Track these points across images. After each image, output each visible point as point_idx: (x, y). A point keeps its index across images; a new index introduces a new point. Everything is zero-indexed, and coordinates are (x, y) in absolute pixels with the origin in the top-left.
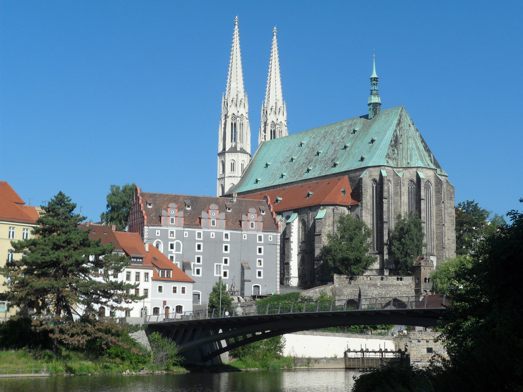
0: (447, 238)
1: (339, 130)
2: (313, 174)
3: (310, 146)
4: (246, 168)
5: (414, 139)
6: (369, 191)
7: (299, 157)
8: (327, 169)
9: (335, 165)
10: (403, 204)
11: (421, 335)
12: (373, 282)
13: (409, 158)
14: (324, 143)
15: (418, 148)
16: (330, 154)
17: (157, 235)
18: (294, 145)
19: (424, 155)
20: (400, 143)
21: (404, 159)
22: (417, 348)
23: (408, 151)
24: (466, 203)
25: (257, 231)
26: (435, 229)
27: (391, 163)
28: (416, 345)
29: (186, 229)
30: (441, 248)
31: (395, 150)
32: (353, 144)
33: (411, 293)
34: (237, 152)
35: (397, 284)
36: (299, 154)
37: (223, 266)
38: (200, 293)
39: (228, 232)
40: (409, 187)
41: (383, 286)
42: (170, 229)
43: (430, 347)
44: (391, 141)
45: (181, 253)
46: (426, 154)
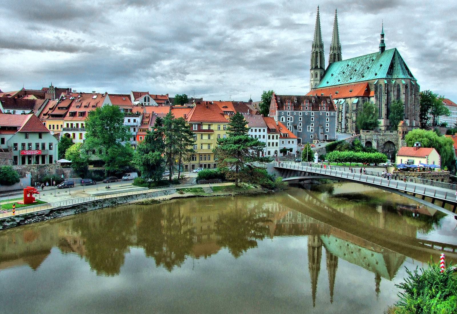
6: (378, 90)
8: (359, 78)
9: (363, 77)
12: (379, 133)
13: (398, 74)
24: (425, 91)
27: (389, 77)
34: (318, 69)
36: (346, 70)
39: (313, 112)
41: (383, 135)
42: (288, 112)
45: (292, 122)
46: (407, 71)
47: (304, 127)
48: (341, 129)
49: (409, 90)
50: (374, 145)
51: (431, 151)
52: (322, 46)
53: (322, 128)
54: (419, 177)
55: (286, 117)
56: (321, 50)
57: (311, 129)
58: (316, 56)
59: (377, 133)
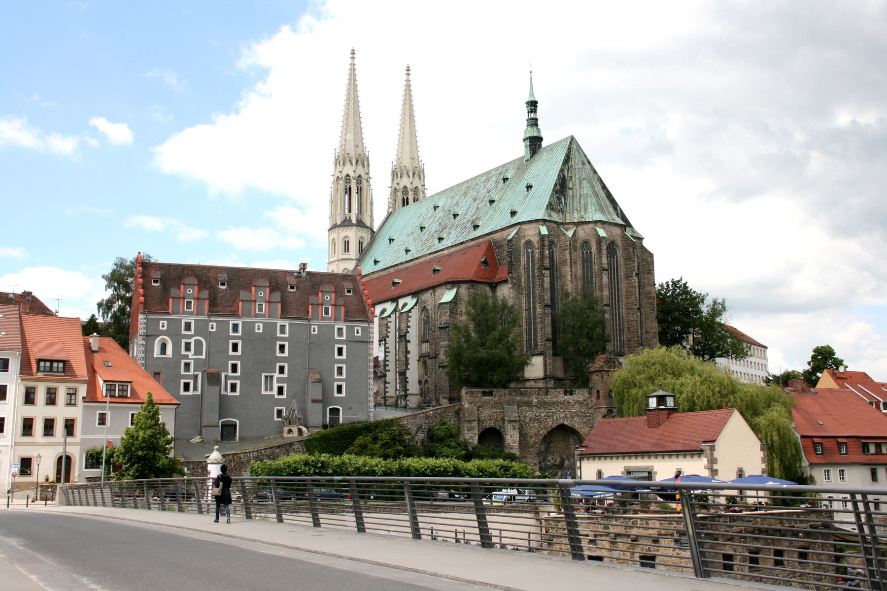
0: (644, 330)
1: (485, 182)
2: (445, 244)
3: (446, 209)
4: (365, 247)
5: (590, 182)
6: (522, 259)
7: (431, 224)
8: (464, 235)
9: (476, 227)
10: (575, 277)
12: (526, 399)
13: (583, 209)
14: (465, 201)
15: (596, 195)
16: (470, 214)
17: (161, 328)
18: (426, 211)
19: (606, 205)
20: (570, 189)
21: (576, 211)
23: (582, 198)
24: (670, 283)
25: (335, 320)
26: (625, 316)
29: (213, 319)
30: (636, 344)
31: (561, 198)
32: (502, 196)
33: (588, 415)
34: (353, 225)
35: (564, 401)
36: (431, 221)
37: (277, 378)
38: (236, 422)
39: (286, 323)
40: (583, 253)
41: (542, 405)
42: (185, 320)
44: (556, 185)
45: (203, 357)
47: (250, 379)
48: (406, 396)
49: (621, 261)
50: (512, 438)
51: (724, 422)
52: (362, 161)
53: (320, 381)
55: (176, 338)
56: (360, 171)
57: (276, 386)
58: (349, 191)
59: (518, 398)
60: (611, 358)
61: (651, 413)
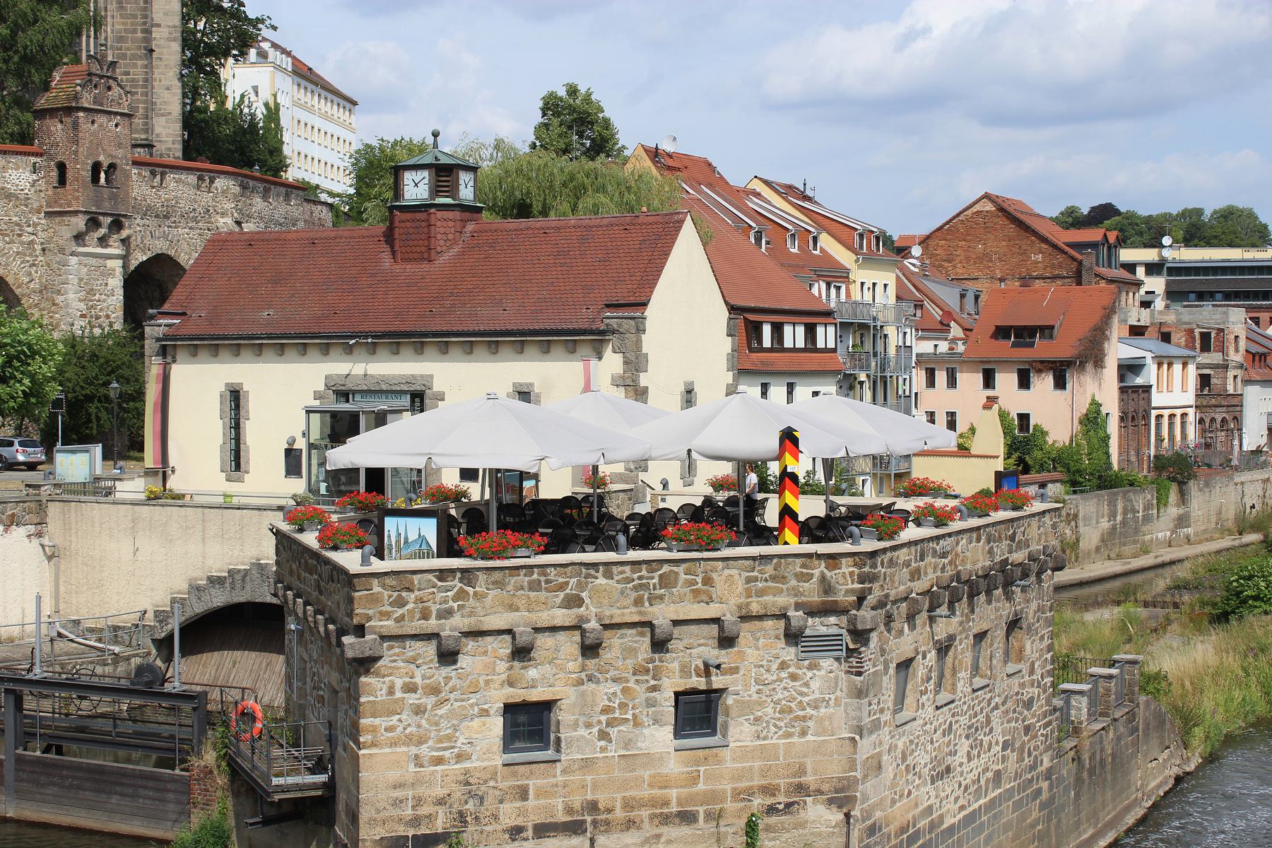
11: (461, 595)
22: (419, 710)
28: (410, 688)
43: (535, 695)
54: (818, 626)
60: (101, 77)
61: (409, 216)
